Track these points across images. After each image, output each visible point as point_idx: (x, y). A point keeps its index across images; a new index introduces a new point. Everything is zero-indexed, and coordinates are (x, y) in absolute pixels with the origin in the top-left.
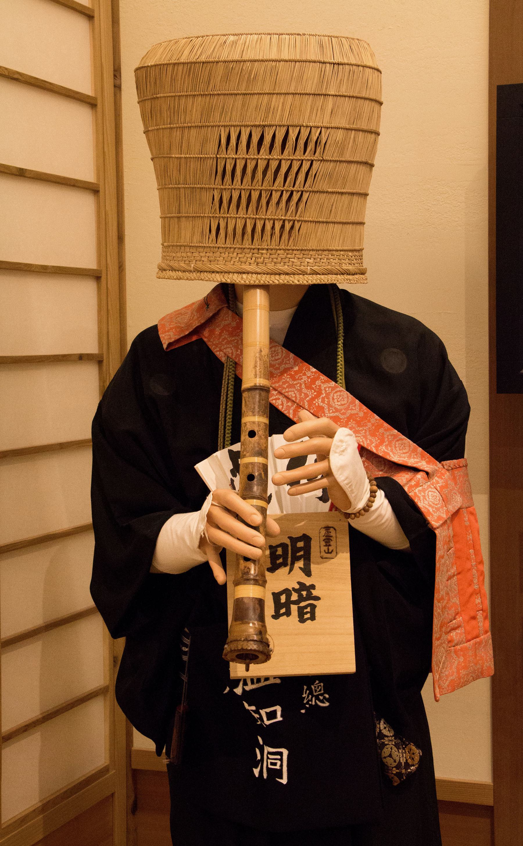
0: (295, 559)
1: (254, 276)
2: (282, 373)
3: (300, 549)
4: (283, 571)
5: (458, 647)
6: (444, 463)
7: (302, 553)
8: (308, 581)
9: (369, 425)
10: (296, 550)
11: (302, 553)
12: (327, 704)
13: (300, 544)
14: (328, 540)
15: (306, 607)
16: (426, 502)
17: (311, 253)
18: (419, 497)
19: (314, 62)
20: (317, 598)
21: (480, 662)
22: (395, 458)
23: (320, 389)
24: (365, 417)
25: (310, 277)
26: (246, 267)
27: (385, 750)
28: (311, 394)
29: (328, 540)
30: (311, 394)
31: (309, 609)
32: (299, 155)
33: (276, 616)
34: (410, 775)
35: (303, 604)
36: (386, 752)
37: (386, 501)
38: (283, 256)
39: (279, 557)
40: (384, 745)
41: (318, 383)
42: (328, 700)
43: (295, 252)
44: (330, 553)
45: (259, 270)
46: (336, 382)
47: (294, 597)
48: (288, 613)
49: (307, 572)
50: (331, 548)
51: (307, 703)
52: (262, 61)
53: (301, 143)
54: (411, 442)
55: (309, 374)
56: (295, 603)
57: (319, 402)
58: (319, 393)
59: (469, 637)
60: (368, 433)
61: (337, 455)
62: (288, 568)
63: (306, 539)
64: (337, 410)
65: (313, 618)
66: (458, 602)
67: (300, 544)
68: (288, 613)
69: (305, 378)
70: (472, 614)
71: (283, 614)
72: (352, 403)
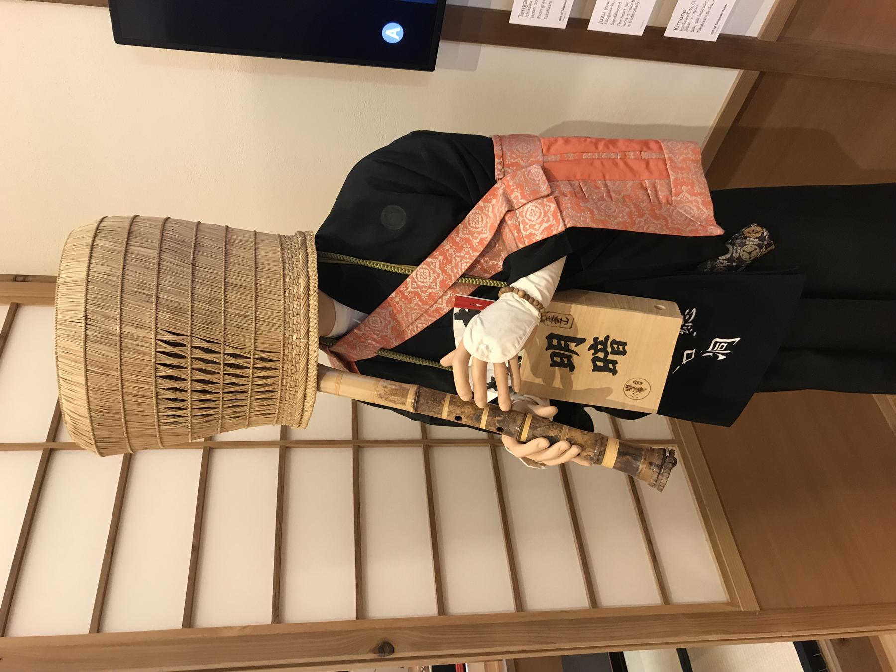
0: (567, 348)
1: (308, 390)
2: (396, 320)
3: (559, 343)
4: (575, 359)
5: (673, 190)
6: (497, 177)
7: (563, 343)
8: (590, 342)
9: (451, 251)
10: (559, 347)
11: (563, 343)
12: (694, 310)
13: (555, 342)
14: (556, 320)
15: (612, 348)
16: (537, 227)
17: (287, 336)
18: (531, 234)
19: (85, 349)
20: (607, 337)
21: (689, 163)
22: (488, 236)
23: (412, 292)
24: (443, 254)
25: (311, 339)
26: (300, 395)
27: (744, 258)
28: (416, 300)
29: (556, 320)
30: (416, 300)
31: (615, 346)
32: (187, 363)
33: (614, 372)
34: (771, 237)
35: (609, 350)
36: (745, 257)
37: (531, 276)
38: (290, 365)
39: (562, 361)
40: (739, 258)
41: (407, 293)
42: (691, 310)
43: (286, 353)
44: (568, 321)
45: (303, 387)
46: (407, 276)
47: (601, 355)
48: (615, 363)
49: (583, 341)
50: (564, 319)
51: (689, 330)
52: (88, 402)
53: (175, 362)
54: (473, 211)
55: (397, 299)
56: (606, 355)
57: (424, 296)
58: (416, 293)
59: (665, 174)
60: (459, 254)
61: (491, 355)
62: (575, 356)
63: (550, 337)
64: (434, 281)
65: (624, 344)
66: (631, 183)
67: (555, 342)
68: (615, 363)
69: (401, 303)
70: (643, 165)
71: (614, 367)
72: (429, 266)
